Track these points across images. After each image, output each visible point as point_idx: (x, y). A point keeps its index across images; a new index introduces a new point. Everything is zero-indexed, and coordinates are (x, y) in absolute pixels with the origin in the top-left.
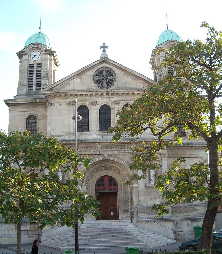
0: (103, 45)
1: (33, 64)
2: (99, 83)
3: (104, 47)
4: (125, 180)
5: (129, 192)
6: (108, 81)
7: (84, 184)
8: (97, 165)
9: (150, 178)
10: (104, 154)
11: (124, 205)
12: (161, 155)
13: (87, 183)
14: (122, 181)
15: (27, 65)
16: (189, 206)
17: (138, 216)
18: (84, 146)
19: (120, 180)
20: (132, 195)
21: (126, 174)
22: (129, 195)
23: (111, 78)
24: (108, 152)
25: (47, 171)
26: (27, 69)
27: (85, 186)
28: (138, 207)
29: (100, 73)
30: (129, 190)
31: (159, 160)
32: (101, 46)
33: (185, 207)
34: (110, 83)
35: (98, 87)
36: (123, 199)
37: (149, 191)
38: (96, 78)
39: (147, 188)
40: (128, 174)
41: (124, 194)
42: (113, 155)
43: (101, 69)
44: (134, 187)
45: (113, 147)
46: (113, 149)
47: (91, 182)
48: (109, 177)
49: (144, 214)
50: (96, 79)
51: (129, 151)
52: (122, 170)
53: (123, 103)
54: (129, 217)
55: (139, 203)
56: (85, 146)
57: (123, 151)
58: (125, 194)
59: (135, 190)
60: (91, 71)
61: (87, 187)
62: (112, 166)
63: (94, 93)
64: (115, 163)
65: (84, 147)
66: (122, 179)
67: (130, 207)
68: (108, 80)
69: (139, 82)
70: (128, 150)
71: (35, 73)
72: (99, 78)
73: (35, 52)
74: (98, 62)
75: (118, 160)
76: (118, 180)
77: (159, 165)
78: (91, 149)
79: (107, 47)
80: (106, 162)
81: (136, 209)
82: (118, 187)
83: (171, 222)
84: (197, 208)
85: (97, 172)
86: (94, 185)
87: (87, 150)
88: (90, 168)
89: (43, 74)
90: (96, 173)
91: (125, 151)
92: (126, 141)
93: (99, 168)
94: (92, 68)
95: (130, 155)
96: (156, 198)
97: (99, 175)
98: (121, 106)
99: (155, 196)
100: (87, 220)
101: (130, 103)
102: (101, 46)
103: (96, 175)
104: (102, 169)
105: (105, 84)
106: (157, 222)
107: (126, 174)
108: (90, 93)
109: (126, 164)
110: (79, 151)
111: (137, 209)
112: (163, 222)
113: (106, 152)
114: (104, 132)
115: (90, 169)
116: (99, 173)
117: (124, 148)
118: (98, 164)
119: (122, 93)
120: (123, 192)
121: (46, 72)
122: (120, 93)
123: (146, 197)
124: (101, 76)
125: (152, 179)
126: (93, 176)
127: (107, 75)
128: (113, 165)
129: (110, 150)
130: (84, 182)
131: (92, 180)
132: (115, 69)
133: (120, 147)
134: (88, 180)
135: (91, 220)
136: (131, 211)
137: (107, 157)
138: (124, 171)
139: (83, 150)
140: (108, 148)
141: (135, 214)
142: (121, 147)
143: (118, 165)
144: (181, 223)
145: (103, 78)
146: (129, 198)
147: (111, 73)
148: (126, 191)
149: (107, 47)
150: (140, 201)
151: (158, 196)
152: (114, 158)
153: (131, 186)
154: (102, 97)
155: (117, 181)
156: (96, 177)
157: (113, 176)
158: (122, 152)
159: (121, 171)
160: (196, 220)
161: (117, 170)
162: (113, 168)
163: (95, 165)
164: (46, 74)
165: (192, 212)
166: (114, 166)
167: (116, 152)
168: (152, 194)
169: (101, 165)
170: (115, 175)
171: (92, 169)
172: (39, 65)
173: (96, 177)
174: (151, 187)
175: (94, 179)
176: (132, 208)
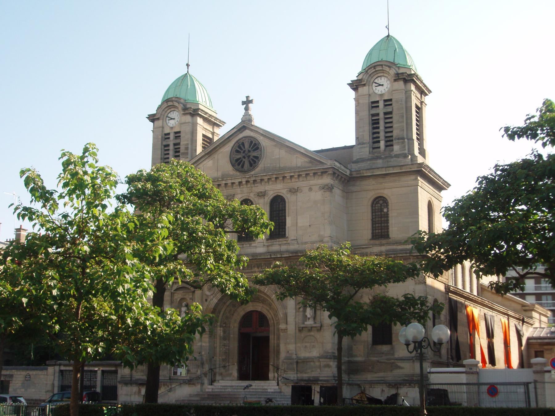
0: (245, 100)
1: (169, 134)
2: (239, 164)
3: (247, 102)
6: (252, 159)
7: (219, 324)
13: (225, 323)
15: (160, 137)
16: (386, 361)
23: (255, 154)
26: (160, 143)
27: (220, 327)
29: (239, 148)
32: (243, 102)
33: (381, 362)
34: (254, 162)
35: (237, 170)
37: (303, 335)
38: (234, 156)
39: (301, 330)
43: (241, 141)
44: (282, 328)
50: (235, 159)
53: (271, 195)
59: (284, 333)
60: (227, 146)
63: (229, 182)
68: (251, 157)
69: (295, 156)
71: (171, 147)
72: (238, 157)
73: (172, 113)
74: (235, 130)
79: (251, 102)
84: (401, 364)
86: (237, 325)
89: (182, 150)
92: (269, 257)
94: (228, 140)
96: (314, 347)
98: (268, 199)
99: (312, 344)
100: (223, 380)
101: (281, 193)
102: (243, 102)
105: (247, 165)
108: (224, 182)
114: (243, 243)
119: (268, 179)
121: (186, 145)
122: (266, 178)
124: (242, 151)
126: (234, 312)
127: (250, 149)
129: (250, 271)
132: (261, 139)
142: (264, 267)
144: (371, 389)
145: (244, 155)
147: (255, 146)
149: (251, 102)
154: (242, 187)
155: (268, 318)
160: (396, 384)
164: (187, 149)
165: (392, 371)
170: (267, 310)
172: (177, 135)
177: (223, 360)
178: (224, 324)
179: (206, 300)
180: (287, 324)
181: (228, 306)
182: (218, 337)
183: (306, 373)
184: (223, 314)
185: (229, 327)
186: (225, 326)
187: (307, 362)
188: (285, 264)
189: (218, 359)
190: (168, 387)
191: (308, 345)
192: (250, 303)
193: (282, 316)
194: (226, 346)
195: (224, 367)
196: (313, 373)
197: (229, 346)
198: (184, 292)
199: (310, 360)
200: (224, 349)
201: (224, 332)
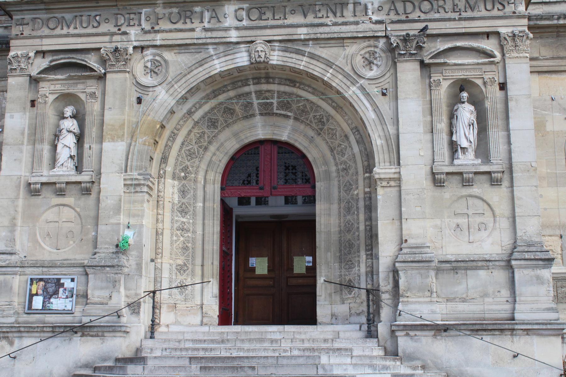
4: (343, 155)
5: (361, 204)
8: (224, 92)
9: (454, 138)
10: (253, 39)
11: (341, 262)
12: (502, 39)
13: (185, 169)
14: (332, 161)
17: (400, 307)
18: (170, 10)
19: (323, 156)
20: (373, 214)
21: (347, 129)
22: (362, 217)
24: (268, 32)
25: (12, 117)
27: (174, 178)
28: (397, 265)
30: (361, 196)
31: (492, 59)
36: (335, 237)
40: (356, 127)
41: (340, 212)
42: (289, 45)
44: (382, 176)
45: (293, 12)
46: (292, 20)
47: (203, 166)
48: (280, 148)
49: (428, 299)
51: (361, 27)
52: (332, 112)
54: (359, 314)
55: (401, 249)
56: (175, 10)
57: (335, 24)
58: (345, 216)
59: (389, 189)
61: (183, 186)
62: (290, 94)
64: (301, 83)
65: (171, 14)
66: (332, 150)
67: (363, 269)
70: (357, 23)
75: (312, 67)
76: (305, 147)
77: (493, 81)
78: (196, 24)
80: (263, 81)
81: (391, 275)
82: (318, 184)
83: (553, 339)
85: (227, 126)
86: (216, 178)
87: (179, 26)
88: (194, 106)
90: (224, 129)
91: (344, 28)
93: (237, 108)
95: (366, 43)
96: (482, 227)
97: (236, 135)
99: (479, 219)
103: (223, 136)
104: (251, 113)
106: (488, 338)
107: (347, 129)
109: (345, 80)
110: (149, 32)
111: (394, 277)
112: (516, 339)
113: (259, 32)
115: (197, 110)
116: (236, 127)
117: (338, 14)
118: (229, 88)
120: (335, 207)
123: (438, 222)
125: (465, 144)
126: (210, 143)
128: (295, 90)
130: (171, 160)
131: (208, 155)
133: (319, 11)
134: (191, 155)
135: (196, 326)
136: (369, 287)
137: (263, 54)
138: (338, 117)
139: (164, 25)
140: (269, 15)
141: (386, 297)
142: (323, 13)
143: (314, 89)
146: (362, 227)
148: (348, 202)
150: (409, 241)
151: (488, 218)
152: (294, 55)
153: (369, 178)
155: (311, 159)
156: (222, 144)
157: (296, 140)
158: (326, 29)
159: (329, 117)
161: (311, 115)
162: (294, 106)
163: (215, 94)
166: (298, 96)
167: (304, 30)
168: (465, 211)
169: (243, 95)
170: (305, 136)
171: (207, 108)
173: (222, 144)
174: (458, 178)
175: (214, 154)
176: (372, 272)
177: (181, 269)
178: (182, 170)
179: (139, 101)
180: (399, 164)
181: (196, 123)
182: (168, 206)
183: (464, 300)
184: (183, 144)
185: (195, 181)
186: (185, 178)
187: (466, 269)
188: (386, 8)
189: (166, 267)
190: (11, 343)
191: (463, 221)
192: (258, 118)
193: (379, 142)
194: (188, 231)
195: (182, 287)
196: (487, 300)
197: (194, 232)
198: (70, 78)
199: (480, 264)
200: (182, 239)
201: (183, 192)
